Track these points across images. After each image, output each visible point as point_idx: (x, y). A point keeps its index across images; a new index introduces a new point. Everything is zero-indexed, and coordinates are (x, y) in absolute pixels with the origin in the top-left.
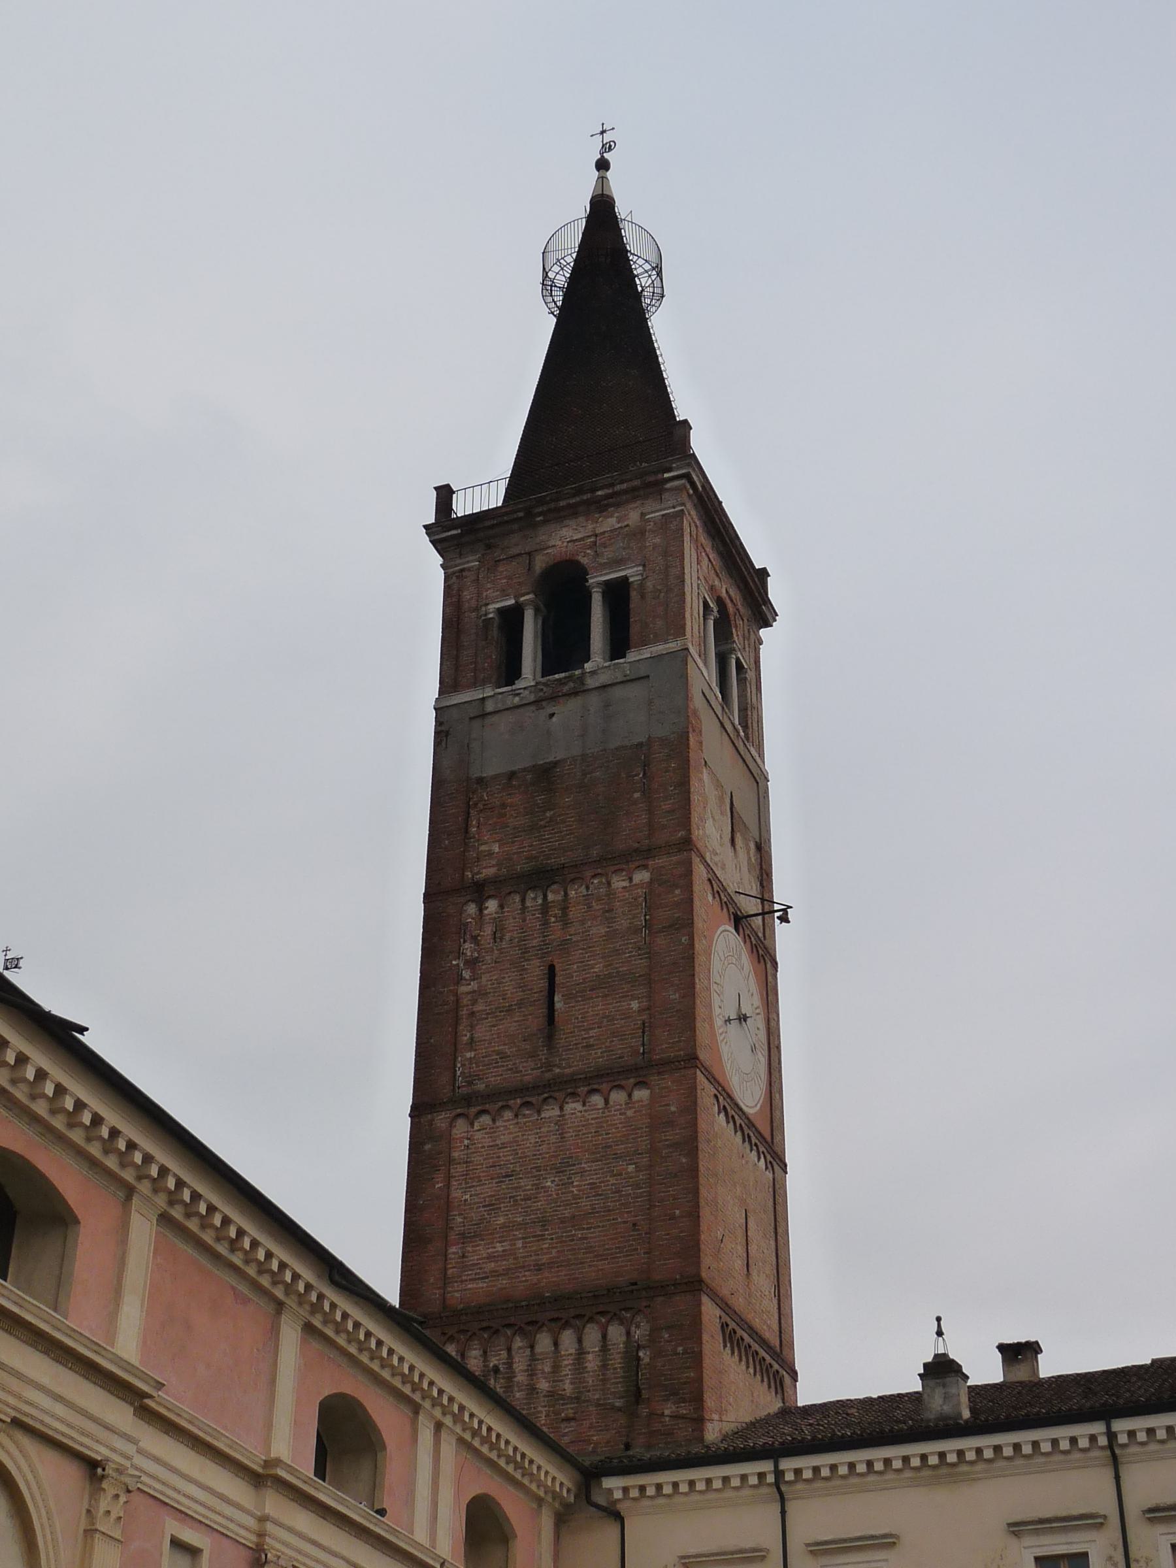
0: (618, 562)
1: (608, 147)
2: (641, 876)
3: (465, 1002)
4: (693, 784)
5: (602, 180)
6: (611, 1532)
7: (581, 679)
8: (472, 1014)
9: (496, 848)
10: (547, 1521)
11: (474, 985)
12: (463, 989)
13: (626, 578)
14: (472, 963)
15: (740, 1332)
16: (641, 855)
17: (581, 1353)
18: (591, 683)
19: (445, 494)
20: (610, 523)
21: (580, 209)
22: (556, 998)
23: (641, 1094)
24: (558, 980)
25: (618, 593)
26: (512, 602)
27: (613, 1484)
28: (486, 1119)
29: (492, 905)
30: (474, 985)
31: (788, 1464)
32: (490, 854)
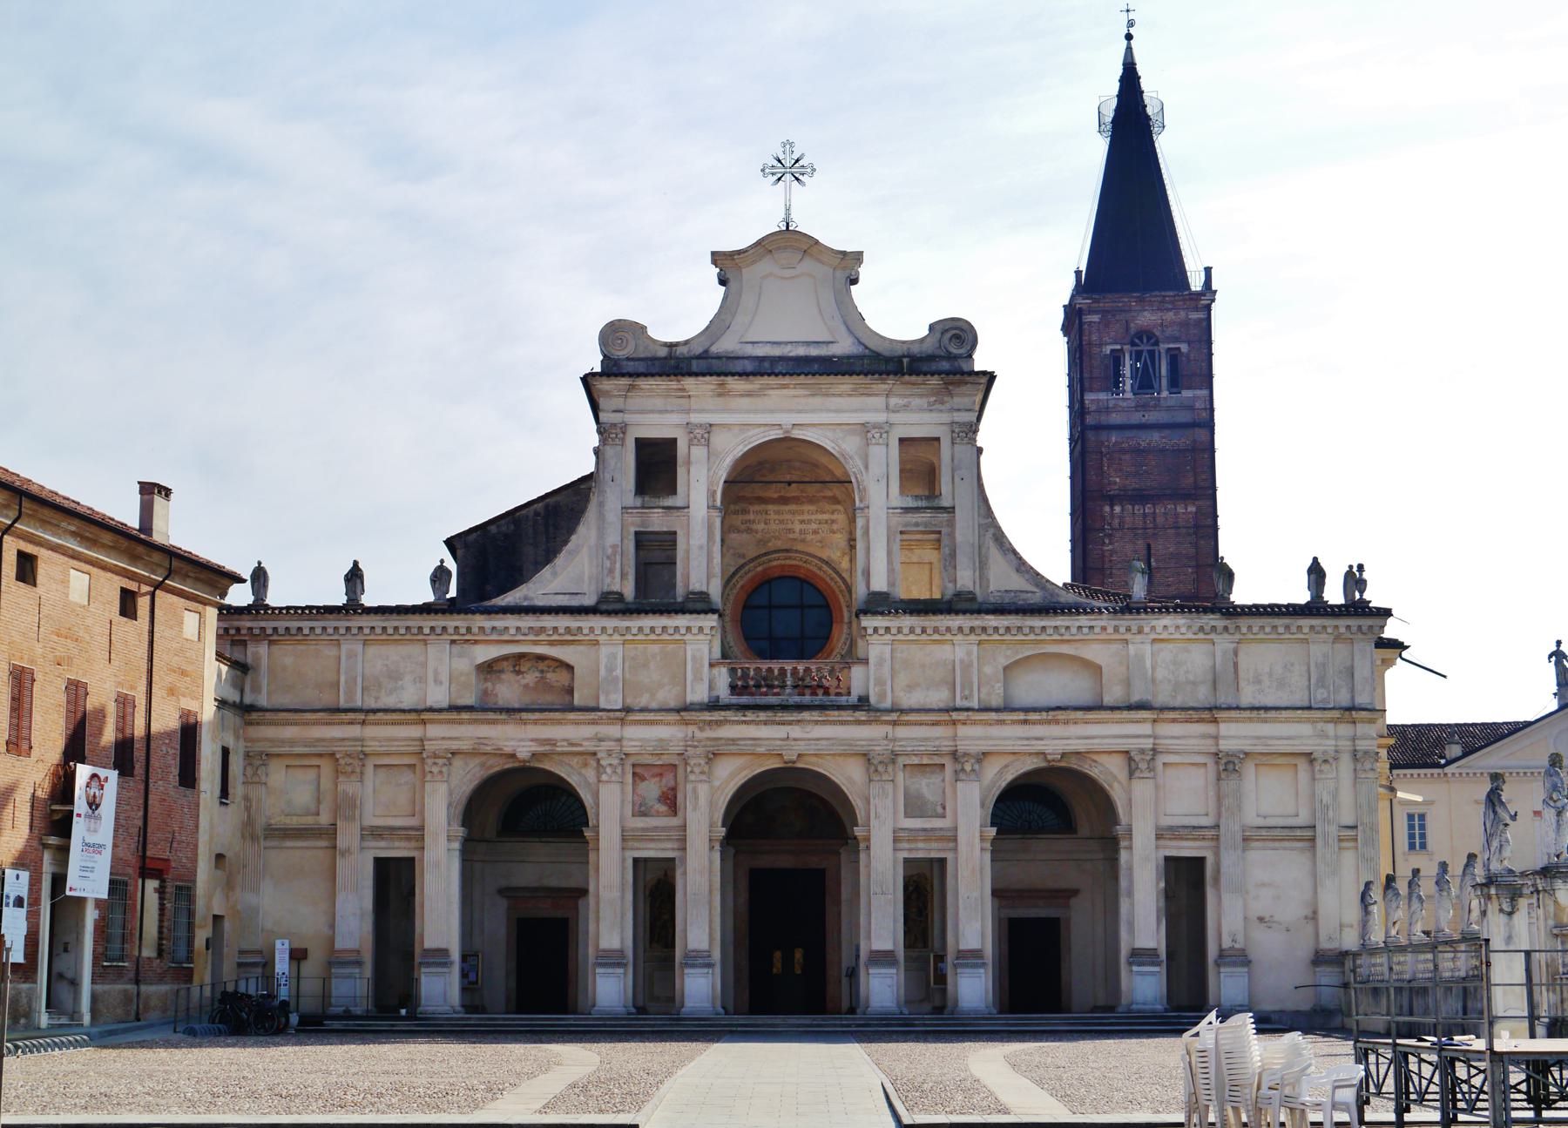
0: (1177, 340)
1: (1131, 24)
2: (1192, 509)
3: (1107, 554)
5: (1129, 49)
8: (1111, 561)
9: (1118, 480)
11: (1110, 547)
12: (1106, 548)
13: (1179, 349)
14: (1110, 536)
16: (1187, 497)
18: (1162, 402)
20: (1170, 316)
22: (1152, 560)
24: (1152, 552)
25: (1174, 357)
26: (1118, 347)
29: (1117, 509)
30: (1110, 547)
32: (1115, 483)
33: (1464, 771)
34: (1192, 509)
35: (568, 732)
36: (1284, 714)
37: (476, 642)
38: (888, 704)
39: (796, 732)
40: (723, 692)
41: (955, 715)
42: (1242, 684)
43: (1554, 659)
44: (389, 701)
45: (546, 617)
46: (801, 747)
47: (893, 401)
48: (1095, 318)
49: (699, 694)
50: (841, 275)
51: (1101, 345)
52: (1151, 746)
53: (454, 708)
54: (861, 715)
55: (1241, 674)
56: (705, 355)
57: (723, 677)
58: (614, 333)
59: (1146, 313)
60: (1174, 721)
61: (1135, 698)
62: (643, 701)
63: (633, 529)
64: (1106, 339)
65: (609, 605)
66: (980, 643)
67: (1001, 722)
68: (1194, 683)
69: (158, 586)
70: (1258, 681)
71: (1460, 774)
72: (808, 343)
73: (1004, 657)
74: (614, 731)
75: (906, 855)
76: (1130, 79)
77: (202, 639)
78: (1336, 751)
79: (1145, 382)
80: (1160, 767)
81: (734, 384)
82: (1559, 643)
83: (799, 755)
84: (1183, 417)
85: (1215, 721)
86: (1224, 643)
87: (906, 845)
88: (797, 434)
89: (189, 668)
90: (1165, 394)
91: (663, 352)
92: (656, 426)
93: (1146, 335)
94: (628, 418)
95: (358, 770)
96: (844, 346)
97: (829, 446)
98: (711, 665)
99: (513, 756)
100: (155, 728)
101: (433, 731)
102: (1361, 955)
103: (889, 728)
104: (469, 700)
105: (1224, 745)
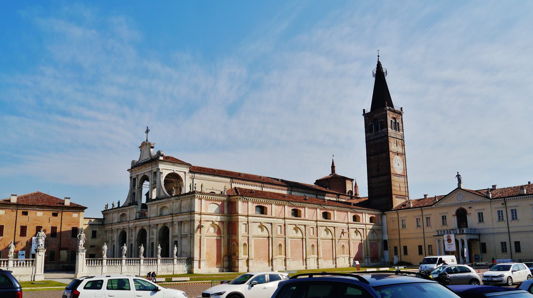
0: (381, 119)
2: (385, 155)
4: (390, 142)
6: (385, 216)
7: (378, 132)
9: (373, 151)
10: (380, 216)
15: (398, 196)
17: (383, 200)
19: (364, 110)
20: (380, 114)
21: (375, 67)
23: (386, 177)
27: (385, 212)
28: (374, 179)
29: (373, 157)
31: (398, 211)
33: (436, 206)
34: (385, 155)
35: (125, 225)
36: (184, 214)
37: (120, 212)
38: (149, 217)
39: (141, 223)
40: (138, 217)
41: (154, 218)
42: (182, 208)
43: (457, 177)
44: (114, 222)
45: (123, 208)
46: (142, 225)
47: (153, 166)
48: (367, 118)
49: (135, 218)
50: (150, 147)
51: (369, 123)
52: (171, 221)
53: (118, 222)
54: (145, 219)
55: (182, 207)
56: (139, 164)
57: (138, 215)
58: (133, 162)
59: (376, 115)
60: (175, 216)
61: (171, 213)
62: (131, 219)
63: (132, 192)
64: (370, 122)
65: (130, 204)
66: (157, 205)
67: (158, 219)
68: (177, 209)
69: (63, 211)
70: (183, 208)
71: (435, 207)
72: (146, 159)
73: (160, 207)
74: (128, 224)
75: (151, 242)
76: (379, 65)
77: (79, 217)
78: (191, 220)
79: (377, 129)
80: (174, 224)
81: (139, 168)
82: (458, 173)
83: (142, 226)
84: (383, 135)
85: (178, 216)
86: (179, 201)
87: (151, 240)
88: (146, 174)
89: (75, 221)
90: (379, 131)
91: (136, 164)
92: (134, 176)
93: (376, 119)
94: (133, 175)
95: (111, 232)
96: (150, 159)
97: (147, 175)
98: (137, 213)
99: (121, 229)
100: (62, 230)
101: (116, 226)
102: (200, 259)
103: (149, 221)
104: (119, 221)
105: (179, 220)
